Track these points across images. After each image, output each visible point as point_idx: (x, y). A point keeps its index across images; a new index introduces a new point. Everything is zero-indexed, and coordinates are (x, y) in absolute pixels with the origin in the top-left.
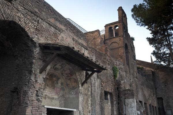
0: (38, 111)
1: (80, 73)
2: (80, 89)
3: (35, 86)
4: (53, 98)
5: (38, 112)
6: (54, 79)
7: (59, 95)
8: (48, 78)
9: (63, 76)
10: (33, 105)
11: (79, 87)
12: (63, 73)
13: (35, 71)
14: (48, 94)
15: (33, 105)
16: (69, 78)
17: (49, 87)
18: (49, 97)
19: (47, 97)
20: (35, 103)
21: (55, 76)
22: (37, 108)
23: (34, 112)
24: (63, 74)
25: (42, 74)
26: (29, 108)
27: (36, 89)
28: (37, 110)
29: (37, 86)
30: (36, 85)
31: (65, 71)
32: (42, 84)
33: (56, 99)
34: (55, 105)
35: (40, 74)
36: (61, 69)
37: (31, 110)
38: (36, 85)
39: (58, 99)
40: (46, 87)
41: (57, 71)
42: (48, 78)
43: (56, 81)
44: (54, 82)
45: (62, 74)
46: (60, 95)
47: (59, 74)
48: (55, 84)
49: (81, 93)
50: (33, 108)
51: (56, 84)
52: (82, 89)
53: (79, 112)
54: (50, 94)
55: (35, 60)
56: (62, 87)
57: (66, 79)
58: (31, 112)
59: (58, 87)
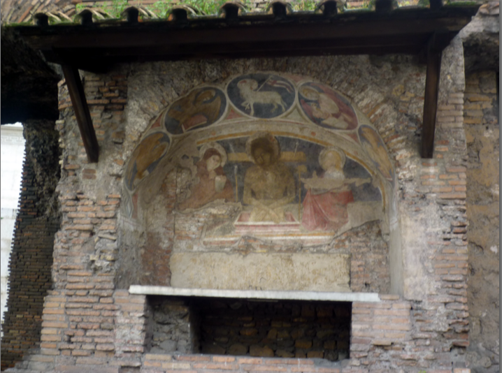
0: (98, 306)
1: (405, 84)
2: (403, 174)
3: (73, 215)
4: (300, 248)
5: (98, 313)
6: (287, 156)
7: (336, 227)
8: (250, 159)
9: (336, 132)
10: (69, 286)
11: (398, 164)
12: (317, 114)
13: (66, 160)
14: (257, 232)
15: (69, 286)
16: (356, 130)
17: (265, 198)
18: (270, 247)
19: (254, 244)
20: (77, 279)
21: (287, 142)
22: (94, 295)
23: (74, 312)
24: (325, 122)
25: (101, 164)
26: (52, 299)
27: (77, 227)
28: (88, 303)
29: (81, 215)
30: (76, 211)
31: (317, 102)
32: (104, 202)
33: (325, 249)
34: (311, 276)
35: (93, 166)
36: (288, 99)
37: (63, 305)
38: (76, 211)
39: (337, 246)
40: (244, 205)
41: (278, 118)
42: (250, 159)
43: (300, 163)
44: (292, 170)
45: (317, 121)
46: (348, 226)
47: (302, 129)
48: (302, 180)
49: (424, 197)
50: (71, 296)
51: (310, 176)
52: (432, 170)
53: (405, 305)
54: (276, 230)
55: (63, 118)
56: (358, 182)
57: (357, 141)
58: (62, 311)
59: (329, 187)
